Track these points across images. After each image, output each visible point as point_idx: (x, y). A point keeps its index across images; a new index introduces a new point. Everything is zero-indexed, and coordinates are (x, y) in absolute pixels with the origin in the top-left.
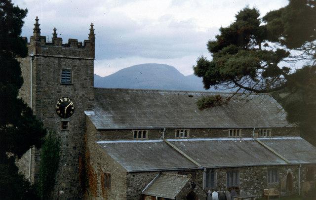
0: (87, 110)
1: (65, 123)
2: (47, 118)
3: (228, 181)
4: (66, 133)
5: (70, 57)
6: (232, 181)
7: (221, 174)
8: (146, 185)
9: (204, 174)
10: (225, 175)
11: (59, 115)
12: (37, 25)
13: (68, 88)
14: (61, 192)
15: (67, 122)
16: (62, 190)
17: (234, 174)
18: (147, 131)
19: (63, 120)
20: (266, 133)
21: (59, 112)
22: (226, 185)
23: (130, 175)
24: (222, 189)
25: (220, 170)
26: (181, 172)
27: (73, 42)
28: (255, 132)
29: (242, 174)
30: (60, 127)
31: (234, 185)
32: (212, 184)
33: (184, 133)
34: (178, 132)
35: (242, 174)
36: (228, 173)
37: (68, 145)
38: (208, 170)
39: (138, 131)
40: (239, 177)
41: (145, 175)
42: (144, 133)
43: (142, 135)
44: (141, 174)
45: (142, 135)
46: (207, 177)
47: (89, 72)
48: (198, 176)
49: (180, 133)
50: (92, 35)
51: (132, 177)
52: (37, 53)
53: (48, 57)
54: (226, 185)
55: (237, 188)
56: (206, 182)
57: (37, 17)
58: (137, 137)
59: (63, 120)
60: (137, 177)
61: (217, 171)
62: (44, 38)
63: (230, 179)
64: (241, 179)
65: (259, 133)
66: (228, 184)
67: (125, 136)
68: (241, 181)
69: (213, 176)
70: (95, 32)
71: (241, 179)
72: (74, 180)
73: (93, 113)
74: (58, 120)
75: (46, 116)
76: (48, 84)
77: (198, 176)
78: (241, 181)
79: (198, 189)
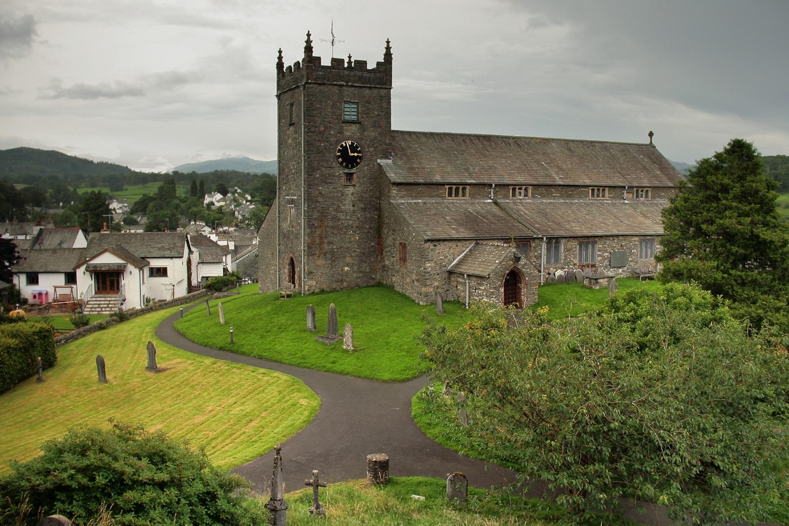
0: (381, 158)
1: (350, 176)
2: (323, 169)
3: (580, 255)
4: (351, 190)
5: (356, 85)
6: (587, 255)
7: (569, 246)
8: (454, 259)
9: (544, 246)
10: (576, 248)
11: (341, 163)
12: (309, 42)
13: (354, 128)
14: (346, 268)
15: (352, 174)
16: (347, 266)
17: (590, 246)
18: (468, 187)
19: (347, 171)
20: (644, 194)
21: (340, 160)
22: (576, 261)
23: (428, 244)
24: (571, 266)
25: (568, 241)
26: (507, 240)
27: (361, 64)
28: (627, 193)
29: (601, 246)
30: (343, 180)
31: (590, 262)
32: (557, 260)
33: (523, 191)
34: (514, 190)
35: (601, 246)
36: (580, 244)
37: (354, 206)
38: (550, 239)
39: (454, 187)
40: (596, 249)
41: (453, 245)
42: (464, 189)
43: (454, 192)
44: (446, 243)
45: (454, 192)
46: (548, 249)
47: (384, 105)
48: (535, 248)
49: (517, 191)
50: (388, 56)
51: (432, 247)
52: (308, 80)
53: (325, 84)
54: (576, 261)
55: (593, 266)
56: (547, 254)
57: (309, 32)
58: (453, 195)
59: (347, 171)
60: (441, 247)
61: (563, 241)
62: (319, 59)
63: (584, 253)
64: (599, 253)
65: (633, 194)
66: (580, 260)
67: (435, 194)
68: (599, 256)
69: (557, 248)
70: (392, 51)
71: (599, 253)
72: (364, 254)
73: (390, 161)
74: (341, 171)
75: (322, 166)
76: (324, 121)
77: (535, 248)
78: (599, 256)
79: (525, 264)
